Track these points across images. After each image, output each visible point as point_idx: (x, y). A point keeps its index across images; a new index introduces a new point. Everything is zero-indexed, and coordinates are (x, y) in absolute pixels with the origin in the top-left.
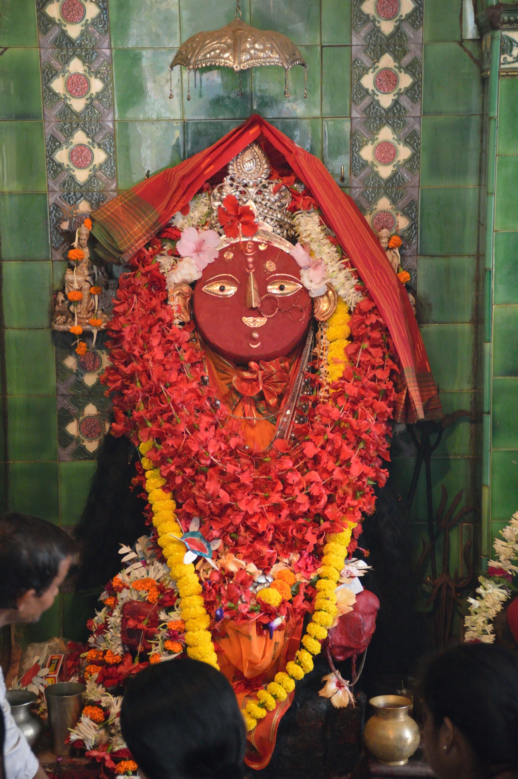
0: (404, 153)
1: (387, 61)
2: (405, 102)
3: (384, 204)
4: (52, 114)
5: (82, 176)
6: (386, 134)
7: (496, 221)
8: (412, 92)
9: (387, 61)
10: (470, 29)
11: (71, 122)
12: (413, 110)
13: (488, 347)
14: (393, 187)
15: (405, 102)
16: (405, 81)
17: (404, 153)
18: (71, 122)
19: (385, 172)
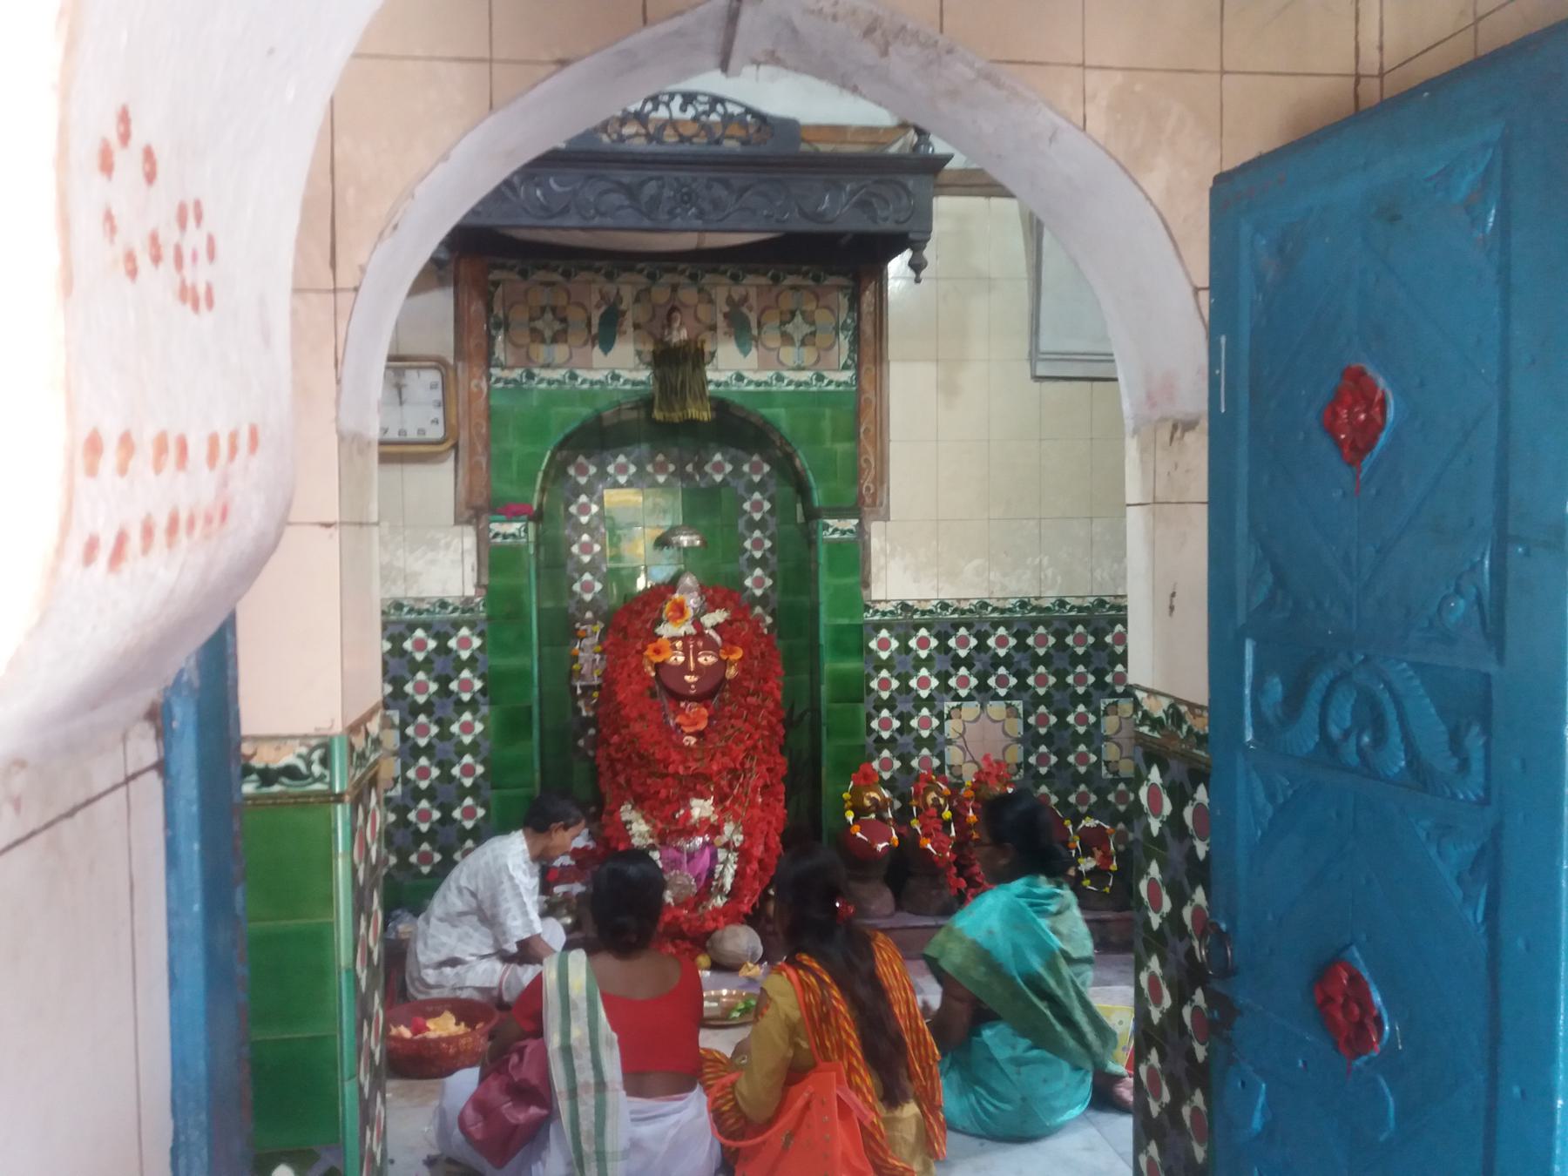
0: (769, 582)
1: (757, 534)
2: (768, 555)
3: (758, 610)
4: (570, 565)
5: (588, 597)
6: (758, 572)
7: (824, 619)
8: (771, 550)
9: (757, 534)
10: (800, 518)
11: (582, 569)
12: (773, 560)
13: (824, 688)
14: (763, 600)
15: (768, 555)
16: (768, 544)
17: (769, 582)
18: (582, 569)
19: (758, 592)
